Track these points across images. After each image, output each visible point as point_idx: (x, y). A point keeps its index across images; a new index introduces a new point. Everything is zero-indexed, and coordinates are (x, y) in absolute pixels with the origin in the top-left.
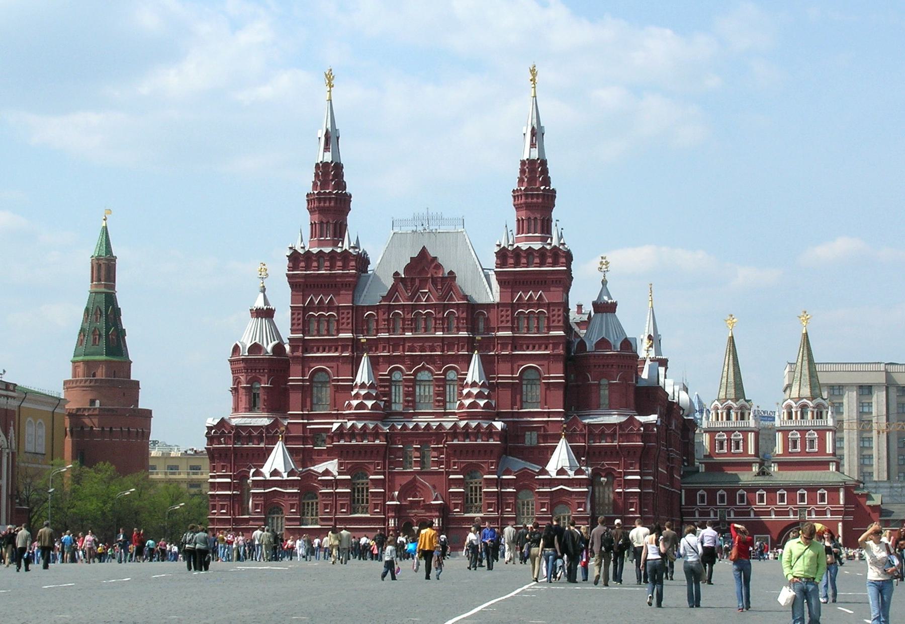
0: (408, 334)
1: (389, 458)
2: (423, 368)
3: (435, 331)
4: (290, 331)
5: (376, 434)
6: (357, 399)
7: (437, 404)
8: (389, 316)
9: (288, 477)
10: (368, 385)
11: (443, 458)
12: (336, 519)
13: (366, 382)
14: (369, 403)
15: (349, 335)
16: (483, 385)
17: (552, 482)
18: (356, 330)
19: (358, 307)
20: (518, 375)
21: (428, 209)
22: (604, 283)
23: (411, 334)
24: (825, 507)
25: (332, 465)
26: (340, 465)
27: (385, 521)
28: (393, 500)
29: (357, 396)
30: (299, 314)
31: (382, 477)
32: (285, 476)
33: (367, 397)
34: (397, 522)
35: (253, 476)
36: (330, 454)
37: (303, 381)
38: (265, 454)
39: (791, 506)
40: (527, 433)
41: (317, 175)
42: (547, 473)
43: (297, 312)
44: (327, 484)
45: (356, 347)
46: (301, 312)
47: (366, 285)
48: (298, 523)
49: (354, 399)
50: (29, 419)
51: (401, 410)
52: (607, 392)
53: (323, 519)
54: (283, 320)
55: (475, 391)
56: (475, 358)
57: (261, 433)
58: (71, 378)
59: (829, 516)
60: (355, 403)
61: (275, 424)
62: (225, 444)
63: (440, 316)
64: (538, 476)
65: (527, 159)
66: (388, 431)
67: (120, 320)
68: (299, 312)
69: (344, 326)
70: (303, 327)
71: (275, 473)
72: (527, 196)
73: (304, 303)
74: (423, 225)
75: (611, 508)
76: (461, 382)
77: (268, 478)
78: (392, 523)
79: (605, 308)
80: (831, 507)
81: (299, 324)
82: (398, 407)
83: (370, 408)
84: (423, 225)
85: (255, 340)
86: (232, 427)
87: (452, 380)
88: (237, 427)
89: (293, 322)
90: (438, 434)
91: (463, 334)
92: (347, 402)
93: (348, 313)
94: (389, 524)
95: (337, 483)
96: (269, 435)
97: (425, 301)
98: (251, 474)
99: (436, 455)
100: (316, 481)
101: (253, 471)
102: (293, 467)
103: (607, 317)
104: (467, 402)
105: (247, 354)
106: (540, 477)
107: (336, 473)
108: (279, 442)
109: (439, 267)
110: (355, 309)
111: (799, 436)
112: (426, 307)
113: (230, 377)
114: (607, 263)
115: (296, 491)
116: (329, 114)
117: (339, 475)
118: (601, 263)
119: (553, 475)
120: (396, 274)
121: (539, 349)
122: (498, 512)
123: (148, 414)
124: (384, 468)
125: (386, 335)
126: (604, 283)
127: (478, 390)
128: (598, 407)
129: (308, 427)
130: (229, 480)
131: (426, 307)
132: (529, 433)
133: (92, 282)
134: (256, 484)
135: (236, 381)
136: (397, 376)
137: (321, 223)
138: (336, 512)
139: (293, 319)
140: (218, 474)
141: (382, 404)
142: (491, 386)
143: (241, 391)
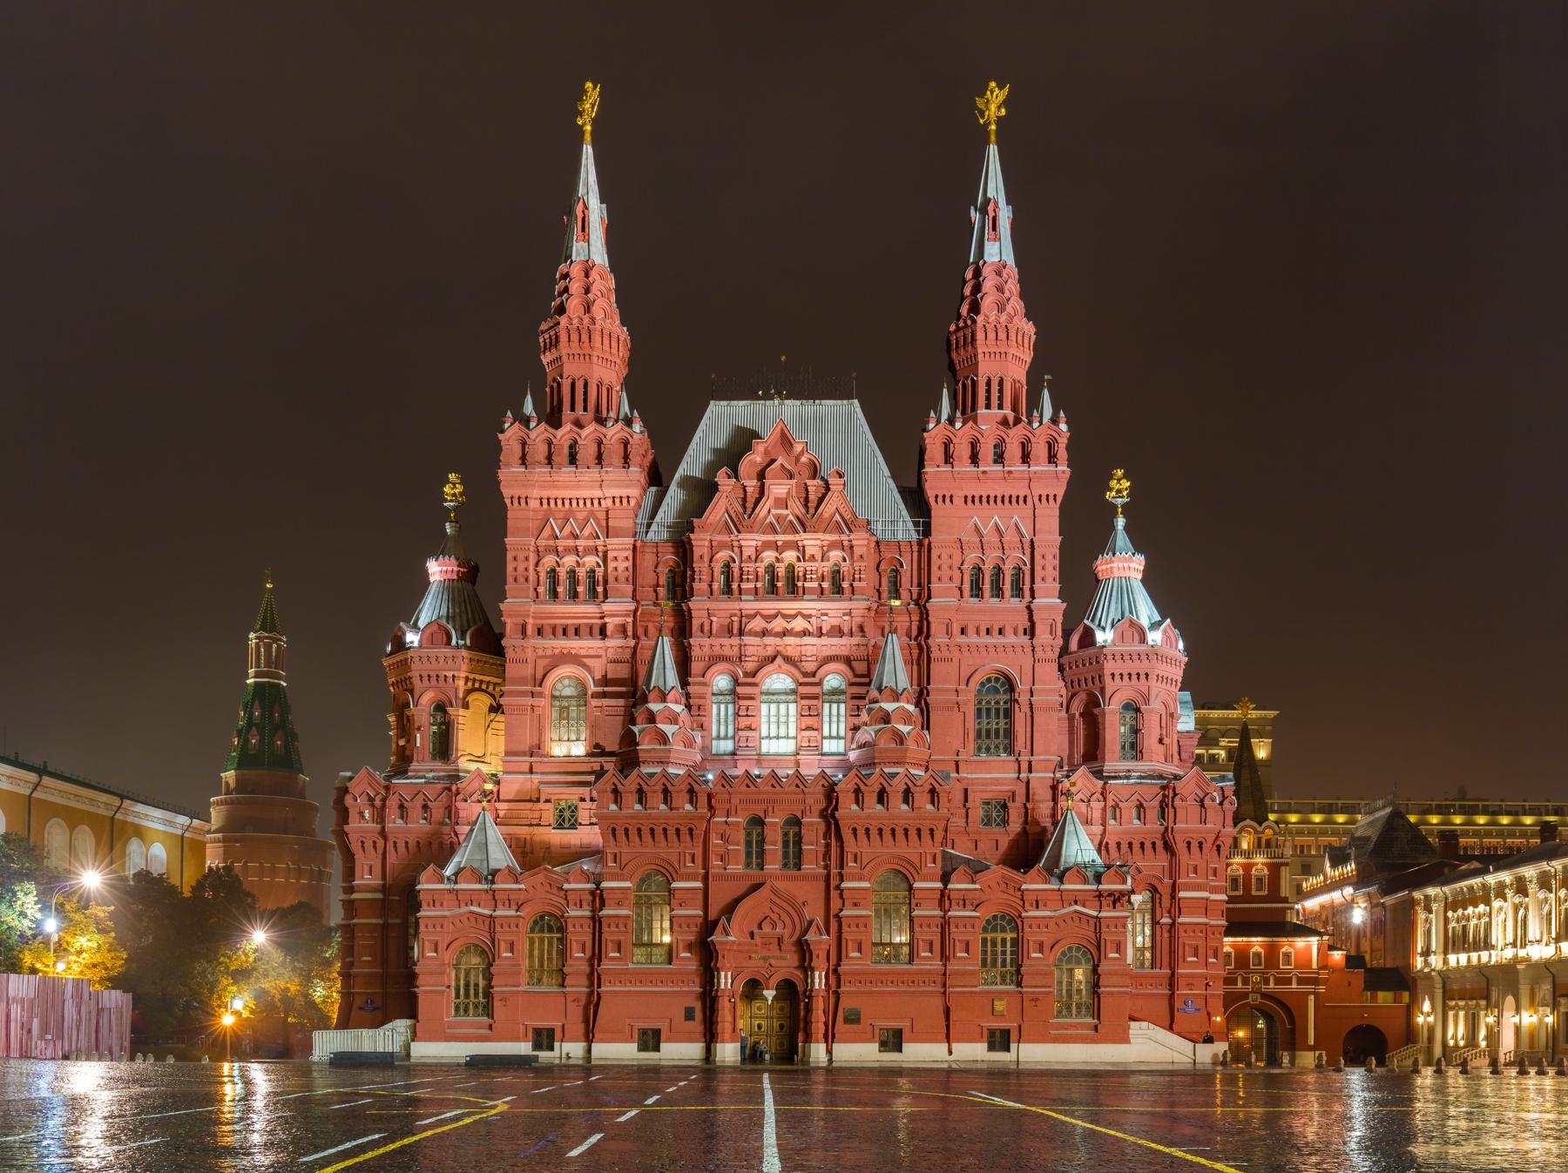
34: (730, 981)
39: (1241, 972)
59: (1294, 986)
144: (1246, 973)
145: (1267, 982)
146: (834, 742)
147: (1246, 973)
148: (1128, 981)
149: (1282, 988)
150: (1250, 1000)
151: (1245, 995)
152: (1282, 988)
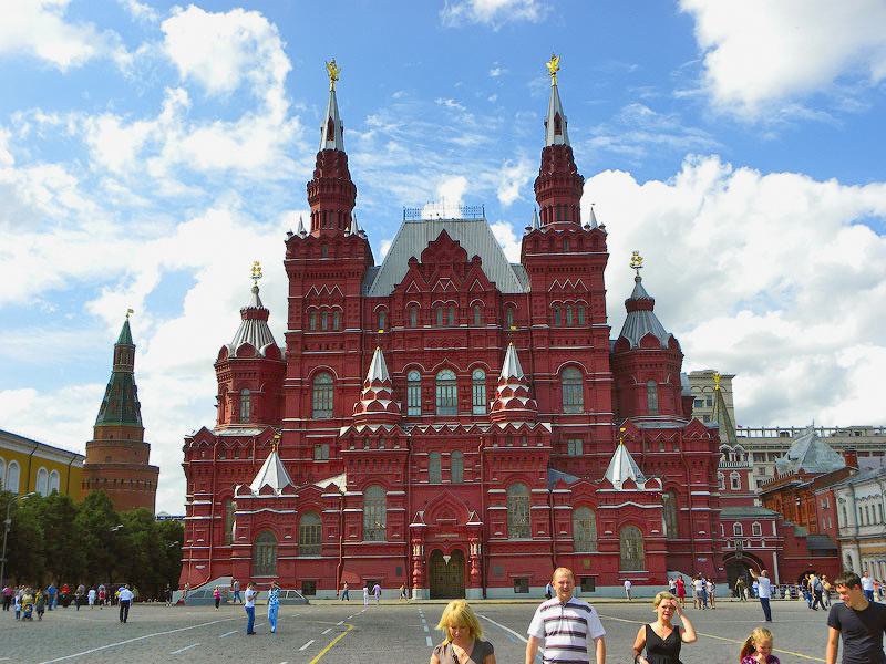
1: (412, 469)
5: (396, 440)
13: (381, 379)
14: (385, 404)
16: (523, 382)
17: (618, 496)
22: (638, 280)
25: (341, 481)
27: (409, 548)
28: (418, 521)
29: (369, 395)
30: (298, 307)
32: (279, 494)
33: (382, 395)
36: (335, 468)
44: (332, 502)
48: (294, 552)
49: (366, 399)
50: (43, 468)
52: (655, 396)
54: (279, 325)
57: (250, 445)
60: (366, 403)
69: (351, 320)
71: (266, 489)
72: (555, 181)
76: (492, 382)
77: (257, 495)
78: (417, 551)
79: (639, 304)
81: (298, 318)
82: (412, 412)
86: (215, 438)
87: (479, 380)
88: (221, 437)
90: (473, 438)
93: (356, 305)
95: (345, 501)
96: (259, 448)
101: (238, 487)
103: (641, 317)
104: (505, 401)
107: (344, 490)
109: (463, 252)
112: (448, 296)
113: (217, 384)
114: (640, 259)
116: (333, 109)
118: (633, 259)
120: (413, 260)
123: (156, 470)
124: (406, 481)
125: (401, 328)
126: (638, 280)
127: (518, 386)
128: (647, 413)
131: (448, 296)
134: (243, 504)
135: (222, 388)
136: (414, 376)
137: (324, 212)
139: (290, 313)
141: (399, 405)
142: (532, 382)
143: (228, 399)
151: (733, 553)
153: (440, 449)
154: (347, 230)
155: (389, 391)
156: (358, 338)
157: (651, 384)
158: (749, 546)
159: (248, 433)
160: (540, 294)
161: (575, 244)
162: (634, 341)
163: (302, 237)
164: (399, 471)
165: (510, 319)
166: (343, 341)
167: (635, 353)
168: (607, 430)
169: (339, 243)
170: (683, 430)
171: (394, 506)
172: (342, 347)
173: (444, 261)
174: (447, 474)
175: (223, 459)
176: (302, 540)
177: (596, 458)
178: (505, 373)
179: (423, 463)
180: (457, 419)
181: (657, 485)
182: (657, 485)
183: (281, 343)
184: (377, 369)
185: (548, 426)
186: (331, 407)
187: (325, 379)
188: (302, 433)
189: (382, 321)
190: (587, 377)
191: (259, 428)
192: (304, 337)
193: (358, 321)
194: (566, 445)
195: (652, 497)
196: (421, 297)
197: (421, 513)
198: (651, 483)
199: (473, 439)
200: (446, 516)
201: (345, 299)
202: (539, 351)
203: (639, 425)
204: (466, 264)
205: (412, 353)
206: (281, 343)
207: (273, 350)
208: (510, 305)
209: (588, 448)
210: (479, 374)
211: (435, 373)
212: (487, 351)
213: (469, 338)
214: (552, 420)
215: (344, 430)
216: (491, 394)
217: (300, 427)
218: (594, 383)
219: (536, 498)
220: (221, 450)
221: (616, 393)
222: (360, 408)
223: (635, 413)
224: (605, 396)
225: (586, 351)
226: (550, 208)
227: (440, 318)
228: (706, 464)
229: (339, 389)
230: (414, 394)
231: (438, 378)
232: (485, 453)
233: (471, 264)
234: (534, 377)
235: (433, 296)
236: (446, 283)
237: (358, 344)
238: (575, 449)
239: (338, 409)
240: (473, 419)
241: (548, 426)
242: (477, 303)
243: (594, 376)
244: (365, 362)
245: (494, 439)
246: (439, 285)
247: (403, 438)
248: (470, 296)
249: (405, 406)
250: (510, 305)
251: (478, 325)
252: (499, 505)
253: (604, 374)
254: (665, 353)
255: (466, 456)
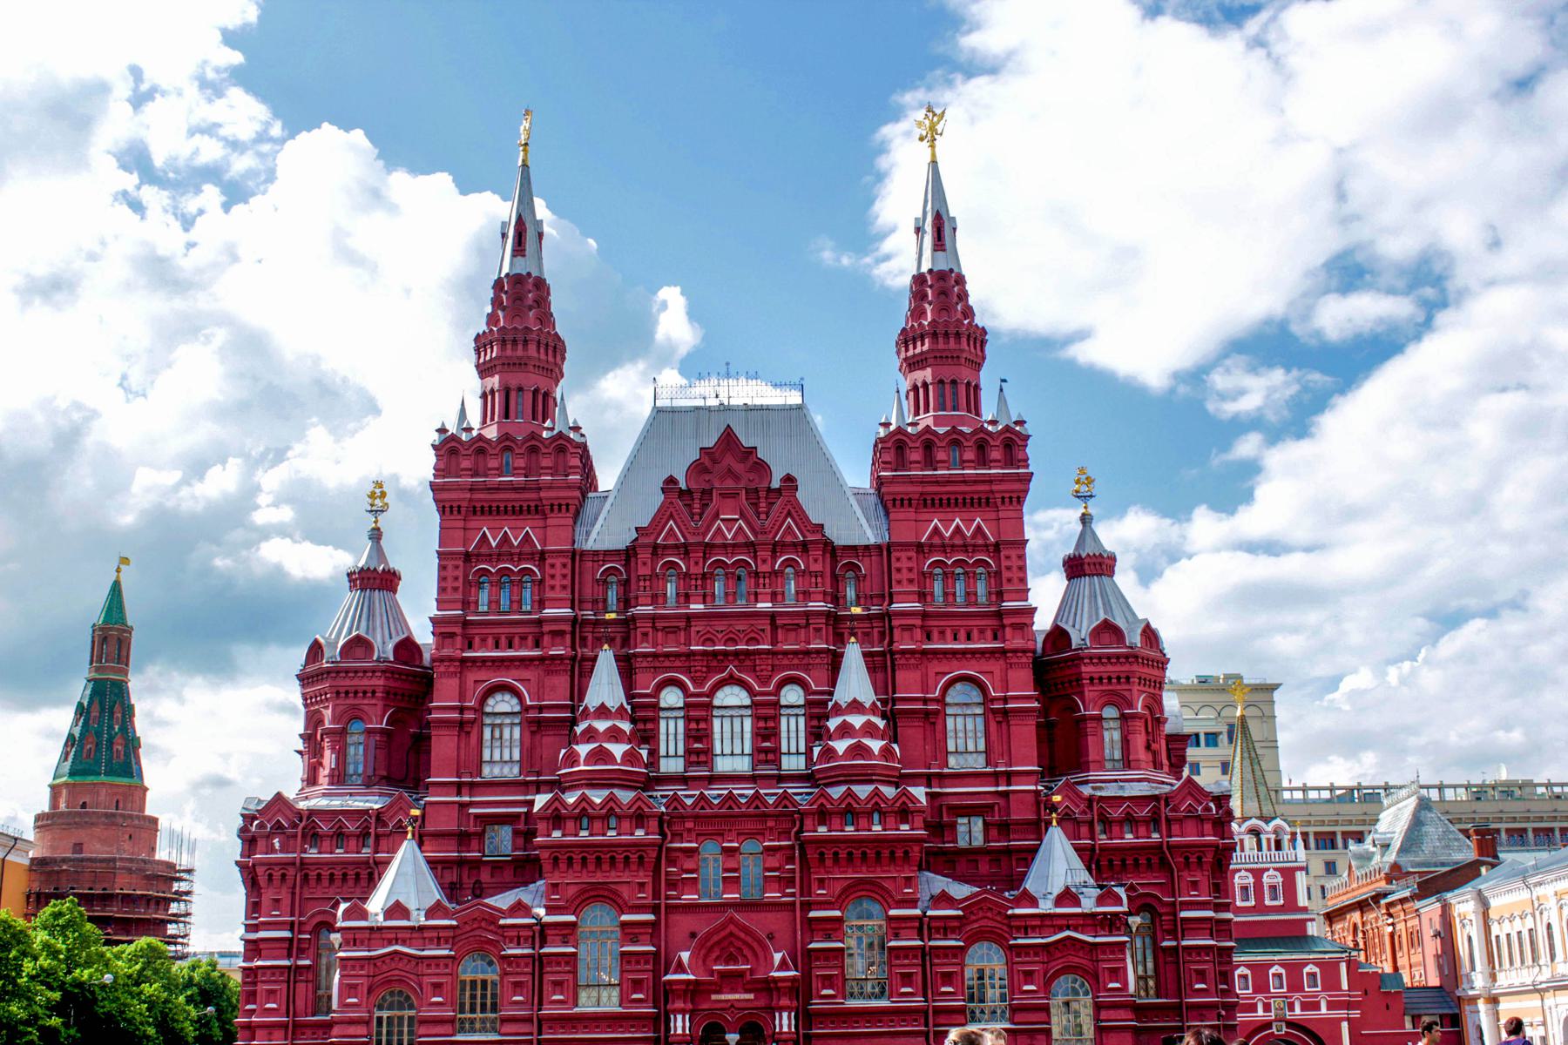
0: (696, 607)
1: (667, 873)
2: (732, 680)
3: (757, 601)
4: (435, 603)
5: (639, 819)
6: (588, 742)
7: (762, 757)
8: (653, 569)
9: (427, 919)
10: (613, 710)
11: (793, 871)
12: (541, 1020)
13: (609, 704)
14: (618, 750)
15: (566, 611)
16: (873, 709)
17: (1047, 922)
18: (581, 602)
19: (583, 553)
20: (937, 694)
21: (728, 364)
23: (702, 606)
24: (1317, 996)
26: (555, 887)
27: (660, 1021)
28: (680, 968)
29: (590, 735)
31: (651, 917)
33: (615, 735)
34: (688, 1024)
35: (344, 920)
36: (523, 870)
37: (462, 710)
38: (371, 875)
39: (1260, 996)
40: (960, 820)
41: (496, 302)
42: (1033, 902)
43: (450, 564)
45: (584, 634)
46: (461, 563)
47: (596, 519)
48: (447, 1028)
51: (680, 768)
53: (505, 1020)
55: (857, 721)
56: (853, 654)
58: (47, 810)
60: (583, 750)
61: (398, 806)
62: (281, 852)
63: (765, 568)
64: (1012, 908)
65: (930, 271)
66: (663, 809)
67: (132, 723)
68: (456, 563)
70: (464, 593)
72: (934, 335)
73: (466, 543)
74: (717, 396)
75: (1151, 983)
76: (817, 712)
80: (1330, 996)
83: (619, 761)
84: (717, 396)
85: (358, 629)
86: (299, 814)
88: (312, 812)
89: (444, 584)
90: (782, 814)
91: (817, 605)
92: (563, 751)
93: (564, 566)
94: (668, 1029)
95: (543, 932)
97: (734, 538)
98: (340, 913)
99: (777, 865)
100: (492, 927)
101: (343, 906)
102: (439, 897)
104: (841, 746)
105: (339, 659)
106: (1018, 911)
108: (406, 842)
109: (762, 468)
110: (578, 557)
111: (1251, 880)
112: (733, 548)
114: (1090, 481)
115: (445, 952)
117: (547, 914)
119: (1046, 907)
120: (671, 481)
121: (982, 638)
122: (925, 995)
124: (656, 895)
128: (1102, 768)
129: (471, 811)
130: (286, 934)
131: (733, 548)
132: (965, 820)
133: (91, 663)
134: (353, 938)
135: (313, 720)
137: (506, 391)
138: (541, 1003)
139: (442, 579)
140: (261, 919)
144: (1266, 998)
145: (1291, 1007)
146: (794, 758)
147: (1266, 998)
148: (1129, 1015)
149: (1311, 1014)
150: (1274, 1030)
151: (1268, 1025)
152: (1311, 1014)
153: (720, 835)
154: (548, 424)
155: (626, 726)
156: (568, 628)
157: (1110, 712)
158: (1298, 1010)
159: (358, 804)
160: (905, 546)
161: (970, 455)
162: (1079, 634)
163: (464, 437)
164: (644, 877)
165: (850, 593)
166: (538, 631)
167: (1078, 659)
168: (1031, 798)
169: (533, 450)
170: (1167, 798)
171: (635, 942)
172: (537, 645)
173: (730, 484)
174: (731, 883)
175: (312, 853)
176: (462, 1005)
177: (1008, 851)
178: (843, 695)
179: (689, 864)
180: (752, 779)
181: (1119, 901)
182: (1119, 901)
183: (424, 636)
184: (605, 687)
185: (919, 792)
186: (517, 756)
187: (502, 704)
188: (464, 806)
189: (612, 596)
190: (994, 700)
191: (381, 795)
192: (466, 624)
193: (567, 595)
194: (953, 826)
195: (1112, 923)
196: (685, 550)
197: (685, 956)
198: (1107, 897)
199: (787, 818)
200: (731, 959)
201: (543, 553)
202: (904, 652)
203: (1086, 791)
204: (769, 490)
205: (667, 655)
206: (424, 636)
207: (407, 648)
208: (852, 567)
209: (994, 832)
210: (792, 695)
211: (712, 693)
212: (808, 653)
213: (774, 627)
214: (928, 780)
215: (541, 800)
216: (816, 733)
217: (459, 794)
218: (1005, 712)
219: (897, 926)
220: (312, 836)
221: (1046, 734)
222: (572, 759)
223: (1084, 766)
224: (1025, 735)
225: (992, 652)
226: (925, 385)
227: (719, 587)
228: (1208, 858)
229: (531, 722)
230: (671, 733)
231: (716, 702)
232: (804, 844)
233: (779, 491)
234: (895, 701)
235: (709, 548)
236: (729, 525)
237: (568, 637)
238: (970, 832)
239: (529, 759)
240: (781, 779)
241: (919, 792)
242: (789, 563)
243: (1005, 700)
244: (581, 670)
245: (823, 816)
246: (719, 528)
247: (654, 816)
248: (776, 548)
249: (654, 753)
250: (852, 567)
251: (790, 605)
252: (828, 938)
253: (1022, 692)
254: (1132, 657)
255: (767, 849)
